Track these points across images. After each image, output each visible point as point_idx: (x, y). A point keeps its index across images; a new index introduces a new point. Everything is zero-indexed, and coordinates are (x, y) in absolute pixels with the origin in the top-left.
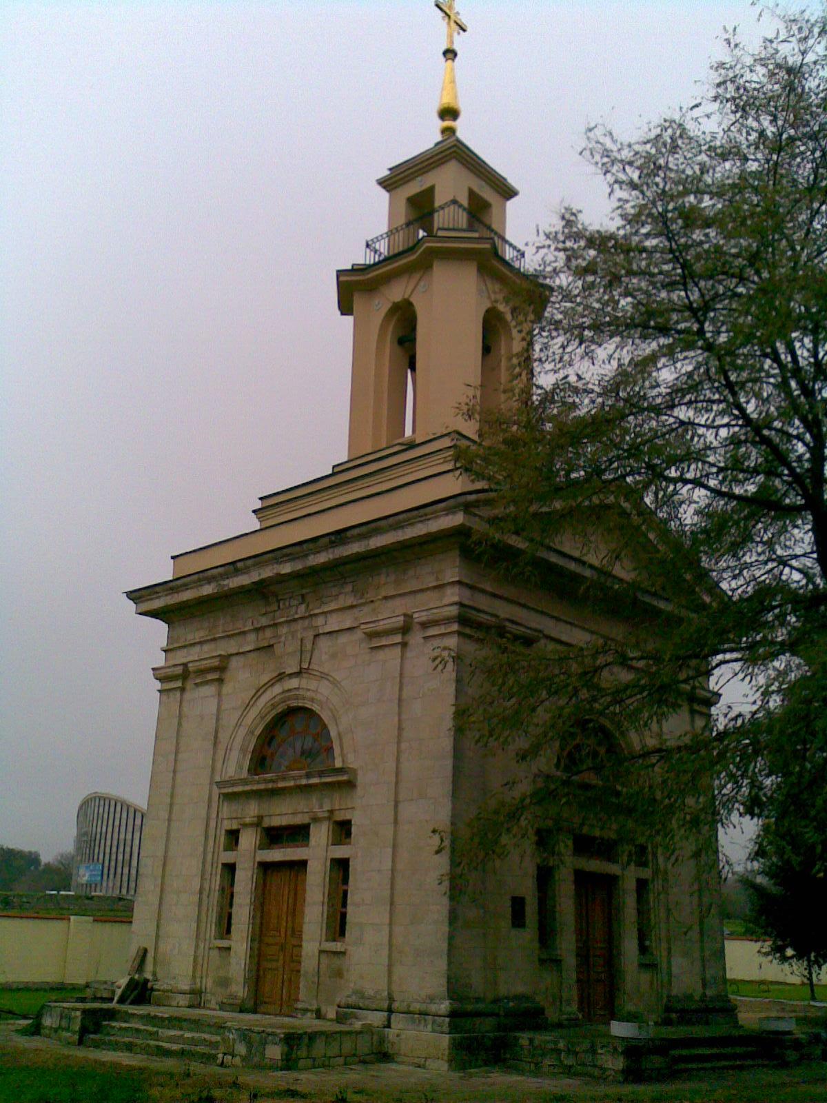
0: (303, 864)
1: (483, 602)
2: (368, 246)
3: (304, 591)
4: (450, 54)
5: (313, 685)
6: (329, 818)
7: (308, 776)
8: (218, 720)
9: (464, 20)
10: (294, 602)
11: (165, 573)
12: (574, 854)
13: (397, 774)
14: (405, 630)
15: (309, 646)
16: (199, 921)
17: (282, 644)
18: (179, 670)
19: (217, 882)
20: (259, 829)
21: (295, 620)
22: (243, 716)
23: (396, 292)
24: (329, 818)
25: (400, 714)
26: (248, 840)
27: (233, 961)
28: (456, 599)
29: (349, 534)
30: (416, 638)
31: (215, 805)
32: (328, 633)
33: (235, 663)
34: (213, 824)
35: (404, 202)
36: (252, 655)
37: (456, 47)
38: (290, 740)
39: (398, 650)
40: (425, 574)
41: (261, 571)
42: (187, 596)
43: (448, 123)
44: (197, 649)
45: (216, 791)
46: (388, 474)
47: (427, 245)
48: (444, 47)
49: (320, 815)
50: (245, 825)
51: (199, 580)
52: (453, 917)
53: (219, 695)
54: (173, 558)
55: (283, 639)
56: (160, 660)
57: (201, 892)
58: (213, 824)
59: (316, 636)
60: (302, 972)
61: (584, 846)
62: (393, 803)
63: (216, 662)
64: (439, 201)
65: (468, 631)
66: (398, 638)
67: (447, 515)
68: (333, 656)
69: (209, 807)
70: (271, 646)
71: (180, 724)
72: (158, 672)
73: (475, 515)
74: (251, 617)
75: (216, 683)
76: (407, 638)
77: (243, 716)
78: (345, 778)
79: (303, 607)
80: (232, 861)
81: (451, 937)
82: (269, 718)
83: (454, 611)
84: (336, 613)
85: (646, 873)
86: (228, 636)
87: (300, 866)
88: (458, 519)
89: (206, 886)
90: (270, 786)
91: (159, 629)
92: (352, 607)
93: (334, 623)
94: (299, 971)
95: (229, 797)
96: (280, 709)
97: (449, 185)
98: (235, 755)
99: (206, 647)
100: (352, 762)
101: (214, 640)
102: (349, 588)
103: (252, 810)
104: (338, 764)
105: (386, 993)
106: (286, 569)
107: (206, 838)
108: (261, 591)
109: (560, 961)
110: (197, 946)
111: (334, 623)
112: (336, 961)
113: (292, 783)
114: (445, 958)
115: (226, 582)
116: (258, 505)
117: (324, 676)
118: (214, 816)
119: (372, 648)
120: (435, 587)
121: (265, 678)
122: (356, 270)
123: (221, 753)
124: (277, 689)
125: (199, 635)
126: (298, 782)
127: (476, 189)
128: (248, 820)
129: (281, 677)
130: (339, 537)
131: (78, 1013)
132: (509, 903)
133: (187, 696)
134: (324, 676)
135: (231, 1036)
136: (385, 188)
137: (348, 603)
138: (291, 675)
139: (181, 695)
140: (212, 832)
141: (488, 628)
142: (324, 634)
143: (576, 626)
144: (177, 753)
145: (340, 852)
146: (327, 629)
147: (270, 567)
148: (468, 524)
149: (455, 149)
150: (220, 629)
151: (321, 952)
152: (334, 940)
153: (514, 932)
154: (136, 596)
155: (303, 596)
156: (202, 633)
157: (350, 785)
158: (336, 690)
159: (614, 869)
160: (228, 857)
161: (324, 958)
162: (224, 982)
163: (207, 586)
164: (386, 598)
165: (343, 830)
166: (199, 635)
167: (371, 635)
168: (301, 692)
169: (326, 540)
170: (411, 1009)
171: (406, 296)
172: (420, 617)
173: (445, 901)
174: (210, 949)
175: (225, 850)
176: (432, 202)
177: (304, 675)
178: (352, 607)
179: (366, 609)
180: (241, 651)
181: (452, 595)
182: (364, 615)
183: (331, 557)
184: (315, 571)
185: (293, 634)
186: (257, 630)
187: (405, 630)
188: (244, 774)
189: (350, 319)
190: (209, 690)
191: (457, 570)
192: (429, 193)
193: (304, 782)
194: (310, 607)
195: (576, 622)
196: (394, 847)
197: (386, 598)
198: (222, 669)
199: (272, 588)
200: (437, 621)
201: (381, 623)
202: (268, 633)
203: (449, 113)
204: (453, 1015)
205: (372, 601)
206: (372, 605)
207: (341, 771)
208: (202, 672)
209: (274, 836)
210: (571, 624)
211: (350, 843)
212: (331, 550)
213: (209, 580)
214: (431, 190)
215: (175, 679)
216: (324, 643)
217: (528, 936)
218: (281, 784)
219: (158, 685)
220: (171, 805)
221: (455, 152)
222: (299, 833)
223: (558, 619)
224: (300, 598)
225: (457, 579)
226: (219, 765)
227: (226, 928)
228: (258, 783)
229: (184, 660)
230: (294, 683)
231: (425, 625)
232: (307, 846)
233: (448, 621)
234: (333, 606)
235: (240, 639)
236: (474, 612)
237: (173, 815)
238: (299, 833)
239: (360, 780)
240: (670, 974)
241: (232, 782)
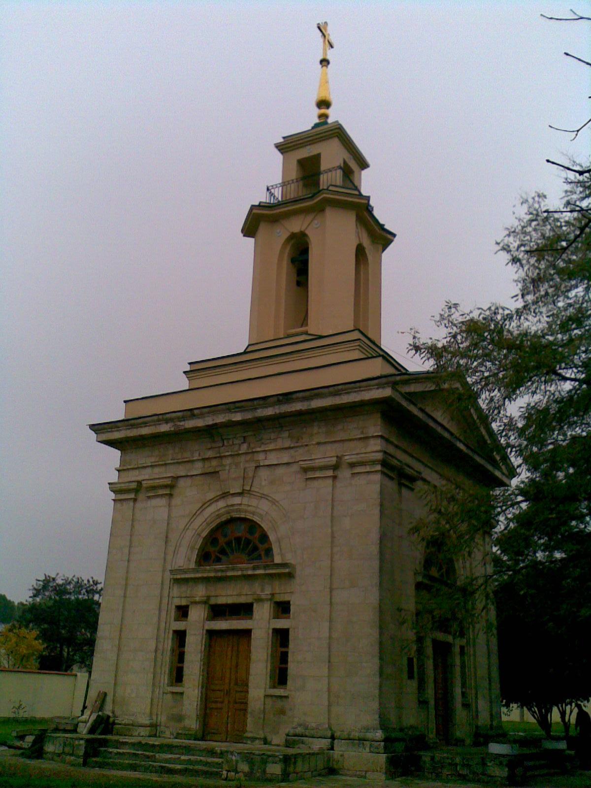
0: (247, 633)
2: (268, 189)
3: (245, 434)
4: (325, 62)
5: (254, 502)
6: (271, 600)
7: (254, 569)
8: (168, 524)
9: (332, 39)
10: (236, 442)
11: (118, 414)
13: (332, 569)
14: (336, 467)
15: (251, 474)
16: (154, 674)
17: (227, 471)
18: (134, 486)
20: (207, 606)
21: (238, 455)
22: (190, 522)
23: (295, 225)
24: (271, 600)
25: (332, 527)
26: (197, 614)
27: (186, 701)
28: (378, 448)
29: (294, 396)
30: (345, 473)
31: (166, 586)
32: (267, 465)
33: (182, 483)
34: (165, 601)
35: (295, 163)
36: (198, 477)
37: (329, 57)
38: (235, 542)
39: (330, 481)
40: (352, 428)
41: (215, 418)
42: (145, 431)
43: (323, 111)
44: (149, 470)
45: (168, 576)
46: (307, 354)
47: (325, 195)
48: (321, 57)
49: (263, 597)
50: (196, 603)
51: (159, 420)
53: (169, 505)
54: (125, 402)
55: (227, 468)
56: (114, 477)
57: (156, 651)
58: (165, 601)
59: (257, 467)
60: (249, 710)
62: (328, 590)
64: (323, 167)
66: (330, 473)
67: (378, 388)
68: (272, 483)
69: (162, 589)
70: (218, 472)
71: (133, 526)
72: (112, 486)
73: (397, 391)
74: (197, 450)
75: (167, 497)
76: (336, 473)
77: (190, 522)
78: (287, 570)
79: (245, 446)
80: (183, 629)
82: (213, 525)
83: (379, 456)
84: (275, 451)
85: (464, 642)
86: (178, 463)
87: (247, 633)
88: (387, 392)
89: (160, 647)
90: (219, 574)
91: (117, 453)
92: (290, 448)
93: (273, 459)
94: (246, 710)
95: (177, 581)
96: (224, 519)
97: (331, 155)
98: (183, 550)
99: (156, 470)
100: (289, 558)
101: (166, 464)
102: (286, 434)
103: (200, 592)
104: (277, 560)
105: (327, 726)
106: (238, 417)
107: (160, 610)
108: (210, 432)
110: (153, 692)
111: (273, 459)
112: (279, 703)
113: (239, 573)
114: (377, 700)
115: (182, 423)
116: (188, 368)
117: (264, 496)
118: (166, 593)
119: (307, 479)
120: (360, 439)
121: (210, 495)
122: (260, 206)
123: (171, 549)
124: (221, 504)
125: (149, 461)
126: (245, 573)
127: (347, 160)
128: (197, 599)
129: (225, 495)
130: (287, 397)
131: (82, 742)
133: (139, 505)
134: (264, 496)
135: (234, 758)
136: (279, 150)
137: (287, 445)
138: (233, 495)
139: (134, 504)
140: (164, 606)
142: (264, 466)
144: (130, 547)
145: (282, 624)
146: (267, 463)
147: (223, 415)
148: (393, 396)
149: (337, 131)
150: (170, 457)
151: (266, 696)
152: (274, 687)
154: (96, 428)
155: (244, 437)
156: (153, 460)
157: (290, 576)
158: (274, 506)
160: (180, 626)
161: (269, 701)
162: (179, 718)
163: (164, 425)
164: (319, 444)
165: (283, 608)
166: (149, 461)
167: (305, 470)
168: (243, 507)
169: (275, 399)
170: (351, 737)
171: (302, 230)
173: (377, 660)
174: (163, 693)
175: (175, 620)
176: (319, 167)
177: (246, 495)
178: (290, 448)
179: (301, 451)
180: (189, 474)
182: (299, 454)
183: (278, 411)
184: (259, 420)
185: (237, 465)
186: (204, 460)
187: (336, 467)
188: (192, 565)
189: (251, 241)
190: (162, 502)
191: (379, 427)
192: (316, 159)
193: (250, 572)
194: (252, 445)
196: (331, 621)
197: (319, 444)
198: (172, 487)
199: (220, 430)
200: (363, 462)
201: (317, 461)
202: (214, 463)
203: (324, 104)
204: (387, 740)
205: (307, 445)
206: (306, 448)
207: (284, 565)
208: (154, 488)
209: (218, 611)
211: (289, 618)
212: (277, 407)
213: (167, 421)
214: (318, 156)
215: (126, 493)
216: (264, 473)
217: (414, 684)
218: (230, 574)
219: (112, 496)
220: (126, 584)
221: (338, 132)
222: (244, 610)
224: (243, 439)
225: (380, 434)
226: (169, 557)
227: (178, 676)
228: (209, 571)
229: (140, 478)
230: (237, 500)
231: (352, 465)
232: (251, 618)
233: (373, 462)
234: (271, 446)
235: (188, 466)
236: (390, 458)
237: (128, 593)
238: (244, 610)
239: (298, 573)
240: (477, 711)
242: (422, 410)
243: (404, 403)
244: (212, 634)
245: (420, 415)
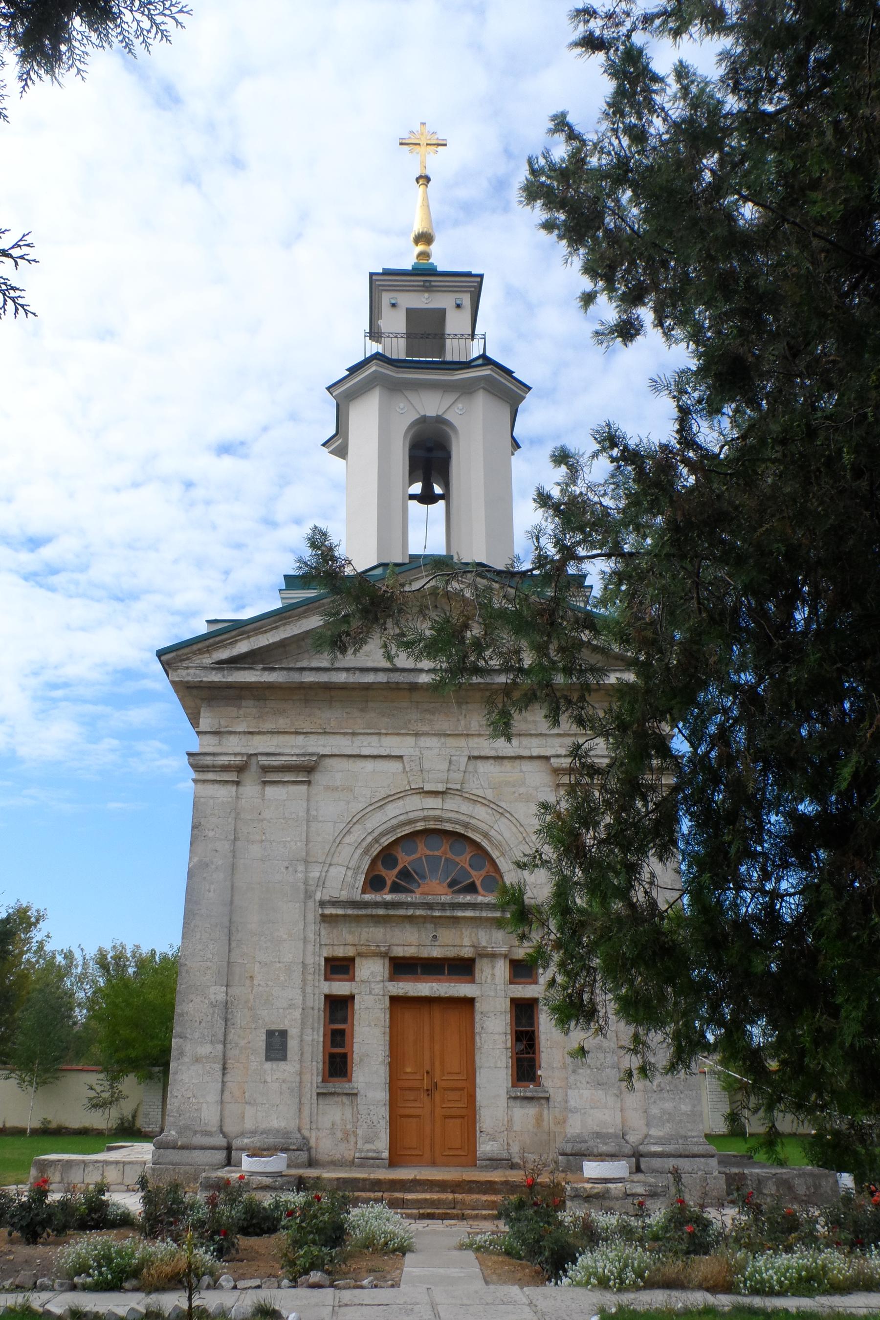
12: (391, 979)
43: (421, 248)
61: (401, 967)
65: (211, 776)
73: (187, 668)
109: (356, 1095)
132: (264, 1037)
141: (241, 769)
143: (386, 734)
153: (268, 1065)
159: (463, 989)
195: (383, 731)
210: (379, 734)
223: (354, 734)
236: (208, 758)
242: (273, 669)
243: (215, 677)
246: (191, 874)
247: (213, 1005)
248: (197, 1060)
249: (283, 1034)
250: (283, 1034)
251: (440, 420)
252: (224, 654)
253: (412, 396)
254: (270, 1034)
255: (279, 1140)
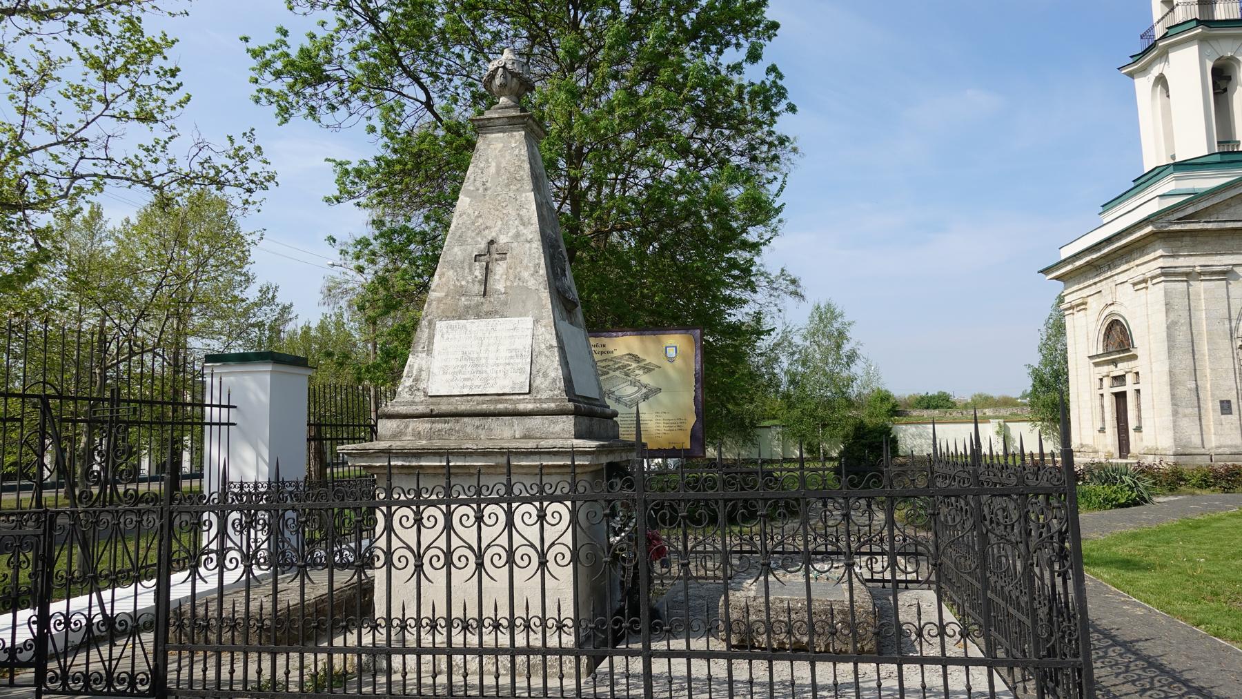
1: (1181, 262)
19: (1098, 403)
23: (1156, 71)
28: (1162, 265)
52: (1175, 413)
63: (1080, 301)
81: (1174, 422)
83: (1159, 271)
87: (1124, 393)
88: (1149, 229)
95: (1096, 364)
129: (1107, 306)
130: (1109, 241)
134: (1122, 304)
145: (1137, 387)
154: (1046, 271)
160: (1101, 392)
167: (1134, 284)
172: (1148, 275)
181: (1161, 263)
208: (1078, 305)
222: (1120, 379)
233: (1159, 276)
241: (1098, 356)
244: (1116, 395)
245: (1210, 226)
246: (1168, 328)
247: (1190, 390)
248: (1185, 416)
249: (1229, 402)
250: (1229, 402)
251: (1232, 58)
252: (1181, 215)
253: (1214, 43)
254: (1222, 402)
255: (1234, 450)
